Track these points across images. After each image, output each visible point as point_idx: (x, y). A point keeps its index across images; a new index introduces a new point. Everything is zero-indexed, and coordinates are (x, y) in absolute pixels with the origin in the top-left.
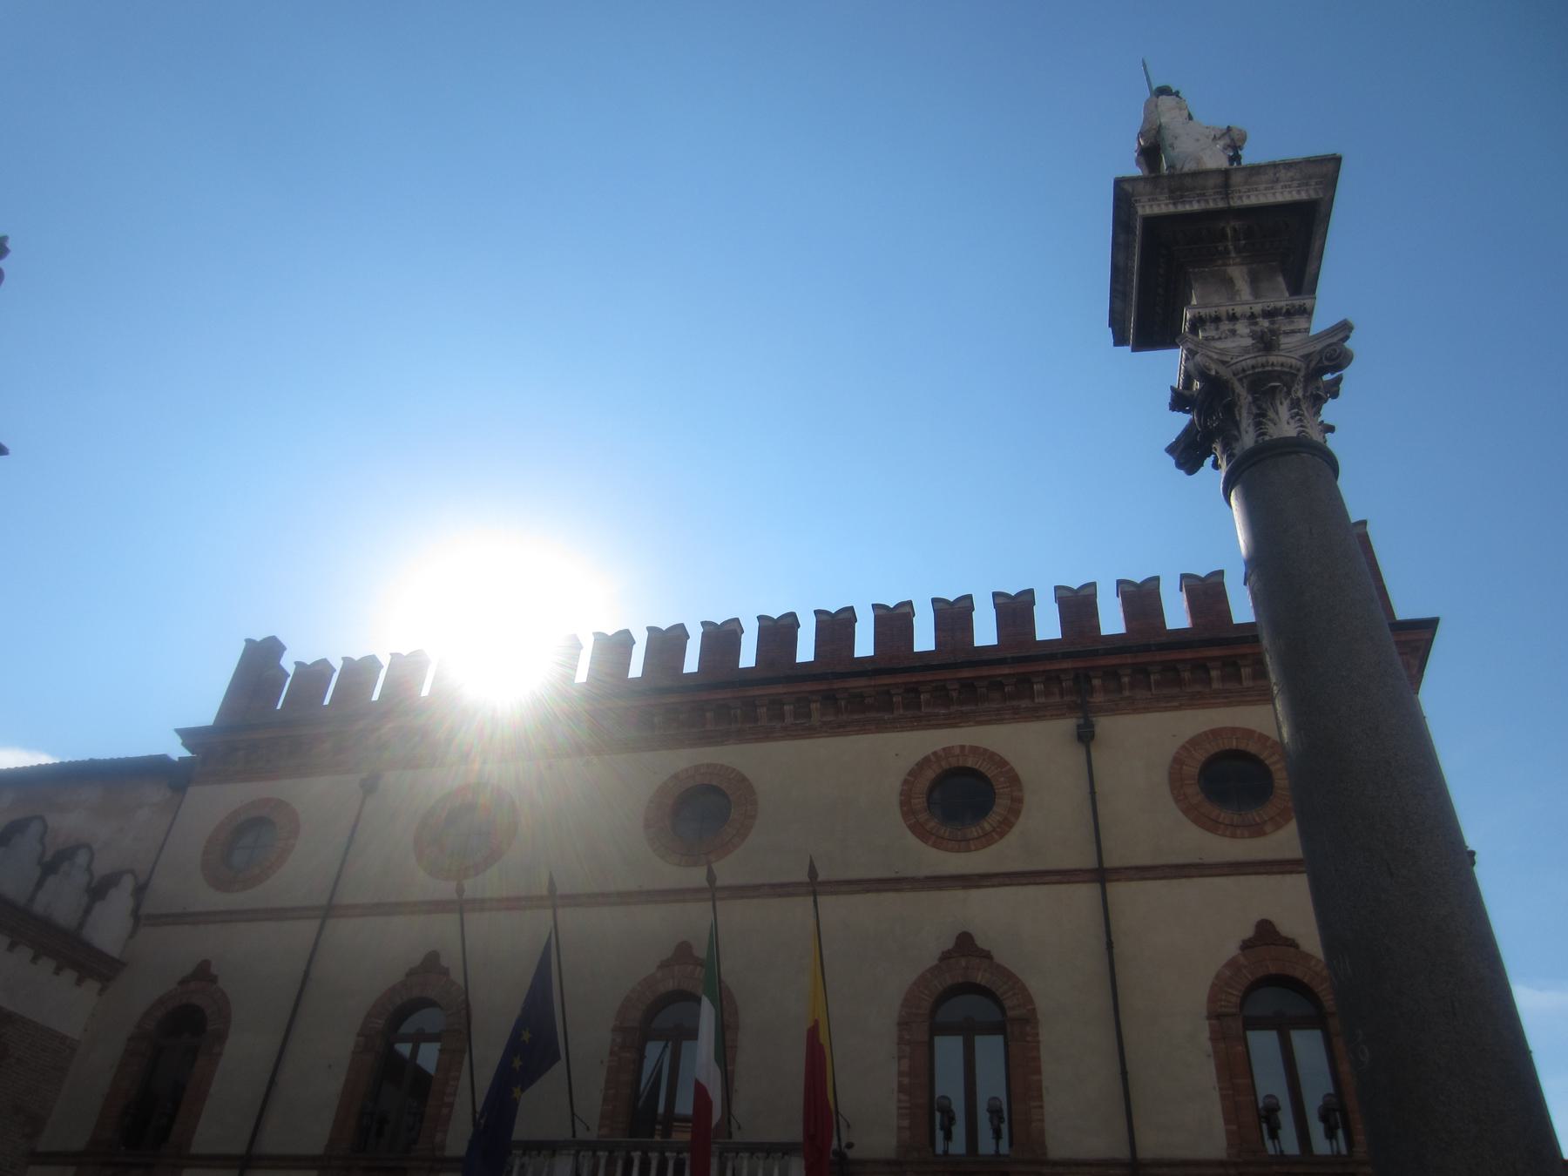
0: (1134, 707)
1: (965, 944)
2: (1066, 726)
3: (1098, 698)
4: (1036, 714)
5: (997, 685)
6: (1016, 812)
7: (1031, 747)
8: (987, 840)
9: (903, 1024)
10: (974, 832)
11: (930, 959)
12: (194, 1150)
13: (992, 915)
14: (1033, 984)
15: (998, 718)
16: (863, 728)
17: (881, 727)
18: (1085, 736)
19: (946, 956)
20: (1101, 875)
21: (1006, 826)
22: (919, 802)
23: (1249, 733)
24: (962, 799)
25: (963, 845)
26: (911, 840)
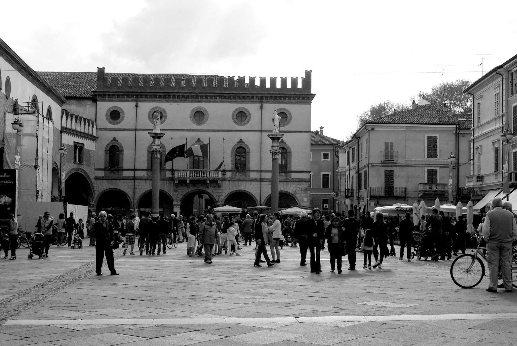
0: (269, 103)
1: (241, 141)
2: (258, 105)
3: (264, 101)
4: (254, 102)
5: (248, 97)
6: (249, 120)
7: (252, 108)
8: (245, 124)
9: (232, 152)
10: (243, 123)
11: (236, 143)
12: (124, 168)
13: (244, 136)
14: (250, 147)
15: (248, 102)
16: (226, 102)
17: (229, 102)
18: (261, 108)
19: (238, 142)
20: (261, 131)
21: (248, 122)
22: (235, 117)
23: (285, 109)
24: (241, 116)
25: (241, 125)
26: (234, 124)
